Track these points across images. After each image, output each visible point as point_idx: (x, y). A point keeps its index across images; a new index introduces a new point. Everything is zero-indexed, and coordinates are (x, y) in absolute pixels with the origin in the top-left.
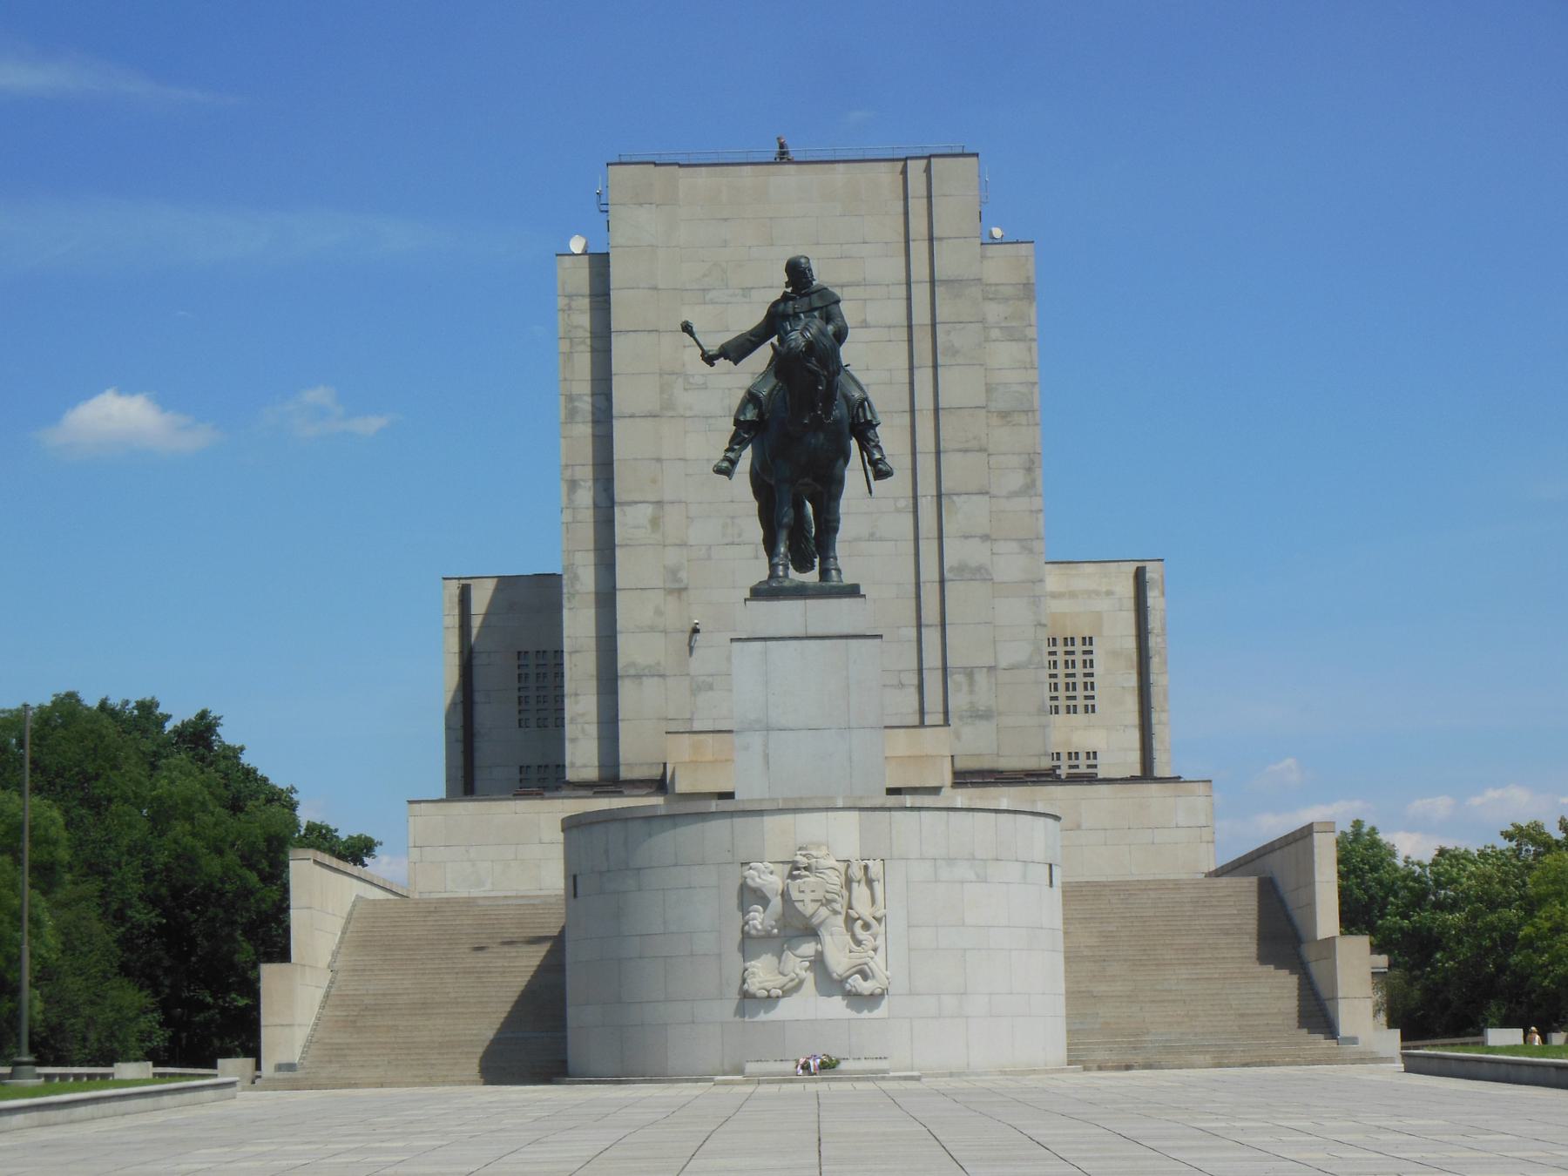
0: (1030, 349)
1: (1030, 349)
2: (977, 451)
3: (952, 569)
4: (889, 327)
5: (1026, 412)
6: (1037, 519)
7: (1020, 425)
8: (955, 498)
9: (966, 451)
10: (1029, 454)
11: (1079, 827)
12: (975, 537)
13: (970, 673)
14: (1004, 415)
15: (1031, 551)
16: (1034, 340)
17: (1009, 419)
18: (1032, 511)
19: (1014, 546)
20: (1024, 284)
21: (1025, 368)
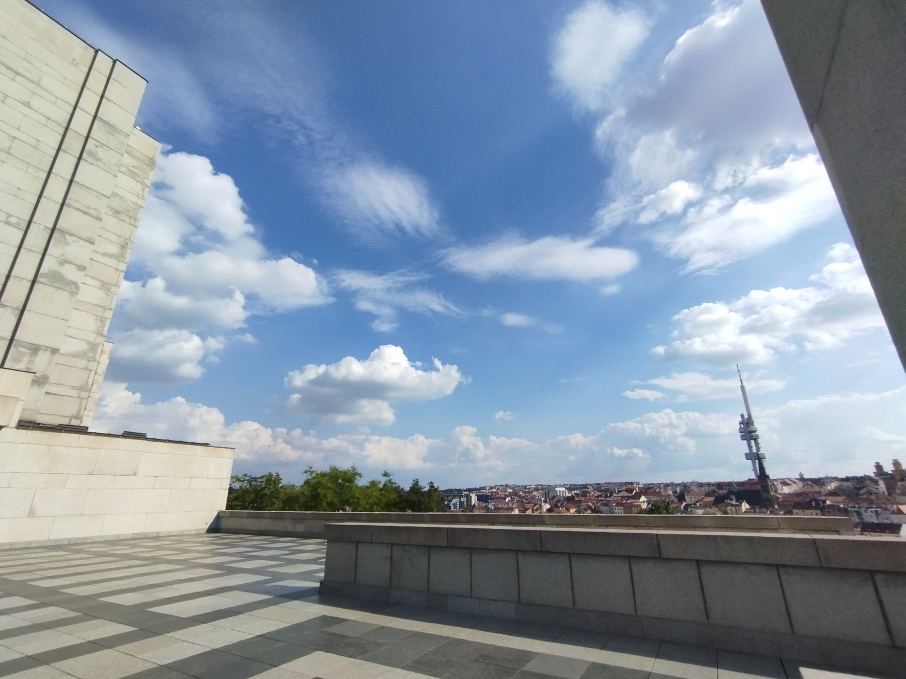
0: (143, 189)
1: (143, 189)
2: (94, 217)
3: (45, 275)
4: (48, 119)
5: (131, 218)
6: (120, 275)
7: (125, 221)
8: (67, 236)
9: (85, 213)
10: (126, 239)
11: (135, 474)
12: (74, 264)
13: (35, 349)
14: (117, 212)
15: (109, 290)
16: (148, 187)
17: (118, 215)
18: (117, 269)
19: (97, 284)
20: (150, 159)
21: (139, 198)
